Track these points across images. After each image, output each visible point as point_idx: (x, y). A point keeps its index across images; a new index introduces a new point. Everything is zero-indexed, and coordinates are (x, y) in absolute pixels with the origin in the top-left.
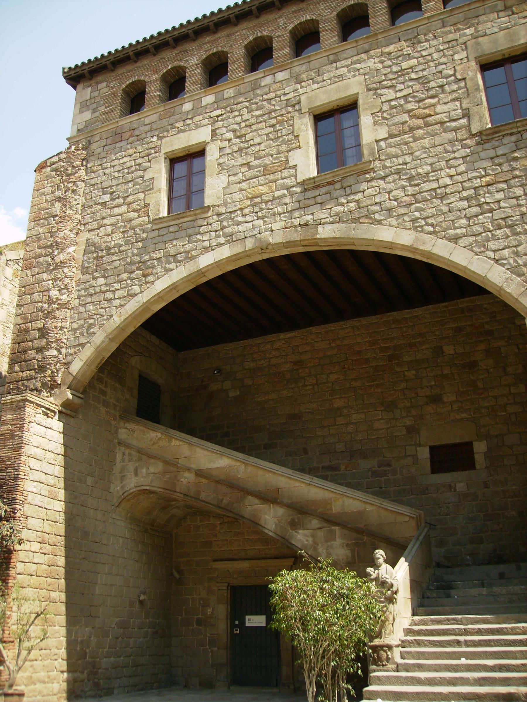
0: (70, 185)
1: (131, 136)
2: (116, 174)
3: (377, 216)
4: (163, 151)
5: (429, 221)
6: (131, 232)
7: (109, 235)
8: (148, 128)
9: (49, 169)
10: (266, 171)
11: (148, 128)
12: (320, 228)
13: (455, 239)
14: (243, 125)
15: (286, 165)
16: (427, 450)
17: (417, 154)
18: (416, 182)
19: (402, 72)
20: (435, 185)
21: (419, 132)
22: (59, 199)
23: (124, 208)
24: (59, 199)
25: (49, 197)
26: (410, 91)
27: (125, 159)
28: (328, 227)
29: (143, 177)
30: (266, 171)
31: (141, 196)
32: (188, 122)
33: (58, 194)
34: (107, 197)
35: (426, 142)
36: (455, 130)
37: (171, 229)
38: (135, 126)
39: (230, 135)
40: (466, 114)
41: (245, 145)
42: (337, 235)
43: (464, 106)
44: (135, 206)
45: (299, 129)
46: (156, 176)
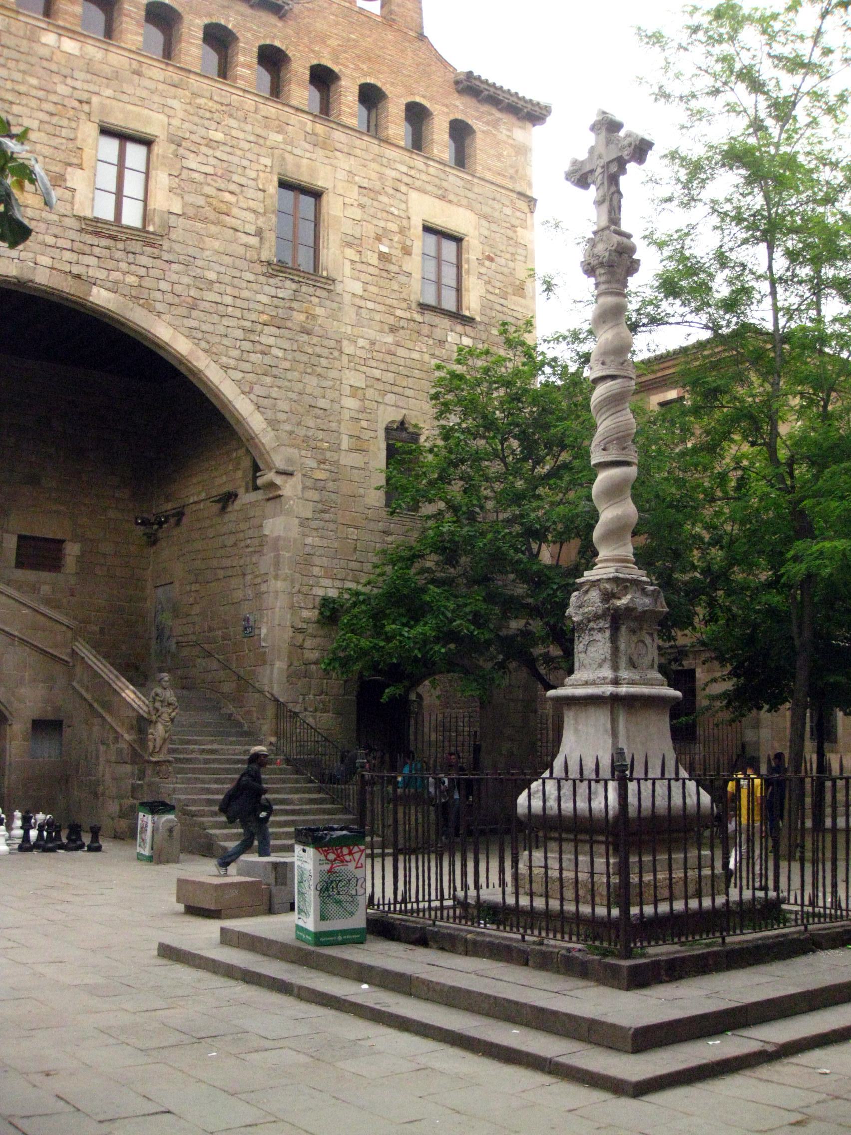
5: (208, 336)
13: (225, 368)
17: (208, 253)
18: (202, 286)
35: (216, 245)
45: (84, 140)
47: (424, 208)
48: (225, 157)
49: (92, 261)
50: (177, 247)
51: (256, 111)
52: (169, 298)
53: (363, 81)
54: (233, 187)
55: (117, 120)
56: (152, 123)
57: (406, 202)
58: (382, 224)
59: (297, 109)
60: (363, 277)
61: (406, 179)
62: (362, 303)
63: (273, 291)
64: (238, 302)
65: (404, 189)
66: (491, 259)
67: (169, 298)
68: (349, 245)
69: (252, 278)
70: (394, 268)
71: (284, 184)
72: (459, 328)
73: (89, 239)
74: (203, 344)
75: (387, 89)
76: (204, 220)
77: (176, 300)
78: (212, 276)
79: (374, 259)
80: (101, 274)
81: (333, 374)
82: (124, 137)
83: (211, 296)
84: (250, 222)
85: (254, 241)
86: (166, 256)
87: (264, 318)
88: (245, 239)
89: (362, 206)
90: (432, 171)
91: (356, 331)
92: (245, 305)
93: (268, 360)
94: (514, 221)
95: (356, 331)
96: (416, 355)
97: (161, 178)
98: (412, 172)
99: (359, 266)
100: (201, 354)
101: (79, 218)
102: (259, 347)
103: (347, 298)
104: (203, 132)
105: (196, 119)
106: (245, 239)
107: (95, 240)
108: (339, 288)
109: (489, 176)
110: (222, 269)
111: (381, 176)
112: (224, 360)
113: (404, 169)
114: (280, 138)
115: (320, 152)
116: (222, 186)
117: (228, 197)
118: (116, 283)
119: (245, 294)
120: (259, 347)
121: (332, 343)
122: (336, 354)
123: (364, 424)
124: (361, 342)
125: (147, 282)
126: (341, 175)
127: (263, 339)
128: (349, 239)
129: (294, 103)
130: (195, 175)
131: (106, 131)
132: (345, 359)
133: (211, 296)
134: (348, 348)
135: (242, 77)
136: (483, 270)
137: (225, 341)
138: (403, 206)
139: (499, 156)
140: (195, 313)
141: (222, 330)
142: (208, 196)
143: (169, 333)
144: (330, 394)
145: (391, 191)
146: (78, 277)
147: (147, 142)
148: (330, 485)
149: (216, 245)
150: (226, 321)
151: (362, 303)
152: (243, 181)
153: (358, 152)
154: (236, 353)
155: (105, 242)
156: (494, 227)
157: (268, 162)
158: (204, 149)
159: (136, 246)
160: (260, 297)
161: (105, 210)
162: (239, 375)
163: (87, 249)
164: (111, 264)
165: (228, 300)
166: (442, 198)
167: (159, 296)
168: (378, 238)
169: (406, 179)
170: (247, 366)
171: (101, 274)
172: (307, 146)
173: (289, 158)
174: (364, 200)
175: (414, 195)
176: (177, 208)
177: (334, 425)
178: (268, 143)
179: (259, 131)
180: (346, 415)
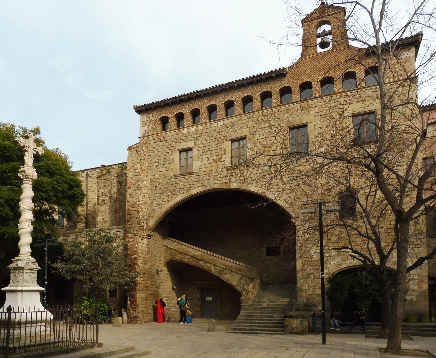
0: (142, 158)
1: (164, 140)
2: (160, 155)
4: (177, 148)
8: (170, 138)
9: (133, 150)
10: (215, 161)
11: (170, 138)
14: (206, 142)
16: (265, 248)
22: (138, 163)
24: (138, 163)
25: (135, 161)
27: (163, 150)
32: (185, 138)
33: (138, 161)
34: (157, 164)
39: (202, 146)
41: (206, 150)
46: (175, 158)
56: (245, 132)
71: (291, 129)
104: (260, 127)
116: (269, 140)
130: (259, 141)
142: (263, 145)
146: (227, 183)
158: (262, 132)
167: (250, 179)
173: (291, 120)
178: (283, 119)
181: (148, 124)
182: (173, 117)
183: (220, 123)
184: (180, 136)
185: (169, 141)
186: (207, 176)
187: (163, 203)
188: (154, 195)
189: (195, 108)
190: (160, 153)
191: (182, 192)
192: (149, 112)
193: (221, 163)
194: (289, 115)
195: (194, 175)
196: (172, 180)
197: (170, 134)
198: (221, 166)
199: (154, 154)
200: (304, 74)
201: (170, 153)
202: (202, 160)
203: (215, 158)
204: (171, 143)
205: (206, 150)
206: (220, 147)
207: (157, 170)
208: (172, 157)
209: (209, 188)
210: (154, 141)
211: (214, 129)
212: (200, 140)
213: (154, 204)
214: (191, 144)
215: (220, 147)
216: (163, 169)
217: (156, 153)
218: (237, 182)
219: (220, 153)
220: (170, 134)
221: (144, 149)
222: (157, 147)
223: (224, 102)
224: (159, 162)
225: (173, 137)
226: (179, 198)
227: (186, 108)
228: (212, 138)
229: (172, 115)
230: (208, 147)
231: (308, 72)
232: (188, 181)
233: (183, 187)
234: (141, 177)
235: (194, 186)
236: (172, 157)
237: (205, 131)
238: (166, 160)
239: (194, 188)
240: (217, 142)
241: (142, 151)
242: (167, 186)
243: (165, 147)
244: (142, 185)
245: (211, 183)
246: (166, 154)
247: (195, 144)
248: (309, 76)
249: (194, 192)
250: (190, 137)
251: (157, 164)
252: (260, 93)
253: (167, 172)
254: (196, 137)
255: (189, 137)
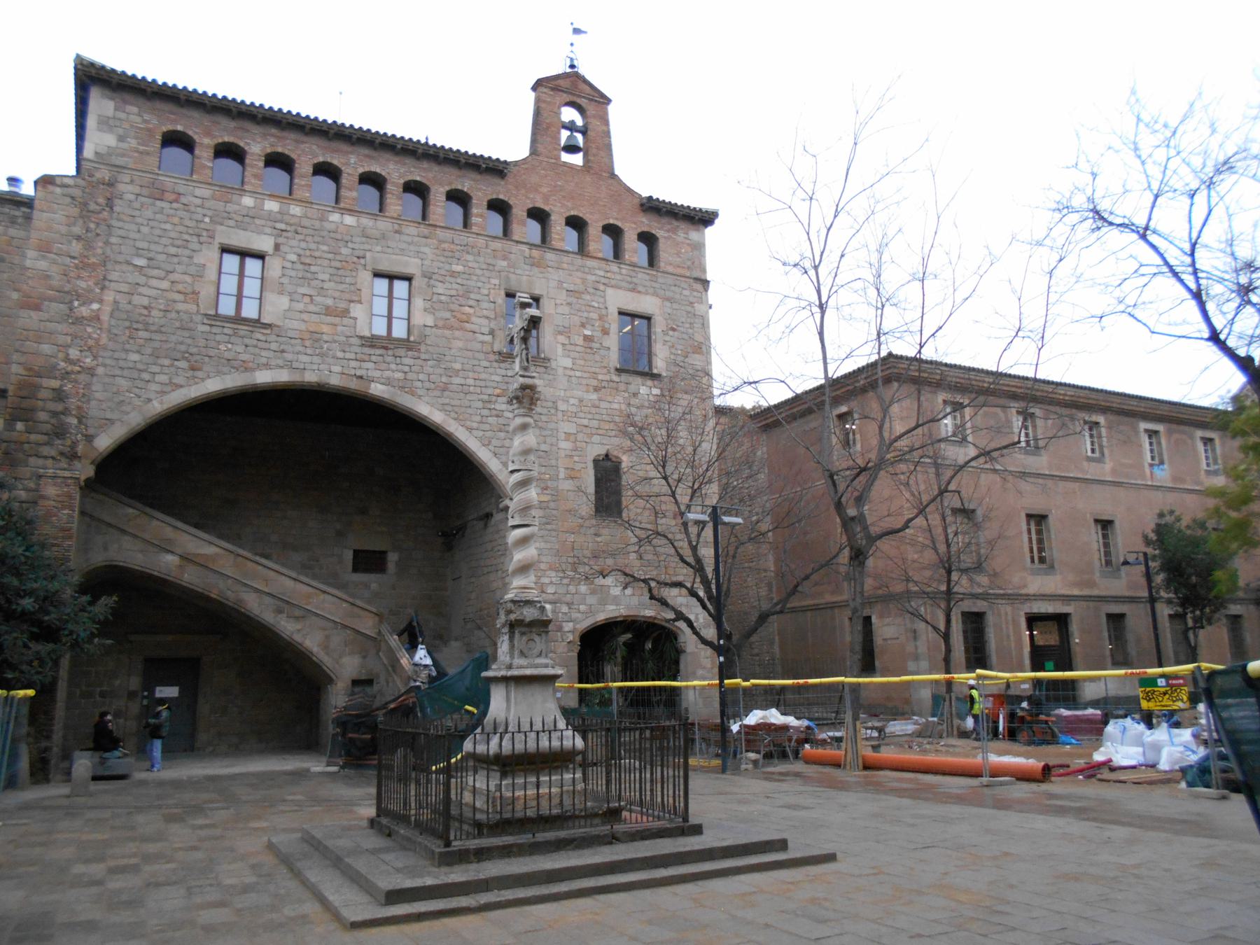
0: (92, 226)
1: (176, 201)
2: (157, 239)
3: (420, 392)
5: (456, 409)
6: (173, 315)
7: (145, 308)
8: (198, 202)
10: (328, 311)
11: (198, 202)
12: (373, 385)
13: (470, 429)
14: (308, 253)
15: (345, 313)
19: (453, 274)
20: (462, 381)
21: (457, 333)
23: (165, 285)
26: (454, 293)
27: (168, 226)
28: (380, 387)
29: (191, 257)
30: (328, 311)
31: (188, 279)
32: (248, 220)
36: (482, 342)
37: (226, 331)
38: (181, 191)
39: (294, 257)
40: (492, 333)
41: (309, 275)
42: (386, 396)
43: (492, 325)
44: (180, 287)
47: (618, 299)
48: (465, 282)
49: (370, 365)
50: (430, 349)
51: (487, 247)
52: (427, 385)
53: (568, 214)
54: (471, 303)
55: (384, 266)
56: (411, 265)
57: (604, 297)
58: (585, 314)
59: (517, 242)
60: (572, 354)
61: (603, 280)
62: (572, 373)
63: (503, 372)
64: (478, 383)
65: (602, 287)
66: (674, 330)
67: (427, 385)
68: (560, 333)
69: (487, 364)
70: (595, 345)
72: (649, 383)
73: (367, 350)
74: (453, 414)
75: (587, 217)
76: (451, 328)
77: (433, 386)
78: (458, 366)
79: (580, 341)
80: (377, 374)
81: (552, 426)
82: (391, 277)
83: (457, 380)
84: (484, 326)
85: (488, 338)
86: (423, 356)
87: (498, 391)
88: (481, 338)
89: (569, 304)
90: (624, 271)
91: (568, 394)
92: (482, 384)
93: (501, 421)
94: (691, 299)
95: (568, 394)
96: (616, 406)
97: (418, 303)
98: (609, 275)
99: (569, 347)
100: (452, 422)
101: (362, 337)
102: (494, 412)
103: (560, 371)
104: (447, 267)
105: (443, 259)
106: (481, 338)
107: (372, 351)
108: (553, 364)
109: (670, 269)
110: (465, 361)
111: (584, 280)
112: (468, 423)
113: (602, 273)
114: (505, 263)
115: (536, 270)
117: (467, 309)
118: (388, 378)
119: (483, 376)
120: (494, 412)
121: (550, 404)
122: (553, 411)
123: (576, 459)
124: (572, 401)
125: (410, 376)
126: (553, 284)
127: (498, 407)
128: (561, 329)
129: (516, 237)
130: (443, 298)
131: (377, 275)
132: (560, 414)
133: (457, 380)
134: (562, 406)
135: (476, 224)
136: (667, 338)
137: (469, 411)
138: (602, 300)
139: (678, 254)
140: (446, 393)
141: (467, 403)
143: (428, 410)
144: (548, 440)
145: (592, 291)
146: (361, 377)
147: (409, 279)
148: (552, 505)
149: (460, 344)
150: (468, 397)
151: (572, 373)
152: (478, 297)
153: (565, 266)
154: (478, 418)
155: (379, 352)
156: (675, 306)
157: (497, 282)
158: (448, 278)
159: (401, 352)
160: (494, 377)
161: (380, 329)
162: (481, 433)
163: (366, 358)
164: (384, 366)
165: (471, 382)
166: (633, 290)
167: (419, 384)
168: (583, 325)
169: (603, 280)
170: (487, 427)
171: (377, 374)
172: (526, 267)
173: (512, 277)
174: (570, 300)
175: (610, 291)
176: (430, 322)
177: (553, 462)
179: (490, 261)
180: (562, 454)
181: (121, 131)
182: (208, 146)
183: (349, 220)
184: (228, 209)
185: (193, 209)
186: (308, 343)
187: (154, 387)
188: (123, 356)
189: (280, 150)
190: (157, 232)
191: (225, 369)
192: (127, 97)
193: (346, 321)
194: (509, 266)
195: (268, 331)
196: (191, 325)
197: (198, 192)
198: (348, 331)
199: (134, 227)
200: (536, 190)
201: (195, 246)
202: (296, 297)
203: (330, 302)
204: (199, 217)
205: (309, 275)
206: (348, 280)
207: (142, 280)
208: (199, 259)
209: (311, 377)
210: (137, 190)
211: (332, 227)
212: (294, 243)
213: (122, 382)
214: (264, 243)
215: (348, 280)
216: (165, 285)
217: (145, 230)
218: (388, 382)
219: (347, 296)
220: (198, 192)
221: (101, 200)
222: (149, 213)
223: (361, 170)
224: (150, 259)
225: (207, 204)
226: (213, 385)
227: (254, 140)
228: (325, 248)
229: (207, 141)
230: (313, 269)
231: (545, 190)
232: (247, 341)
233: (227, 355)
234: (83, 284)
235: (264, 360)
236: (199, 259)
237: (306, 222)
238: (176, 260)
239: (267, 366)
240: (338, 264)
241: (92, 206)
242: (173, 338)
243: (176, 220)
244: (84, 311)
245: (315, 367)
246: (179, 243)
247: (277, 247)
248: (546, 198)
249: (264, 378)
250: (263, 222)
251: (141, 262)
252: (448, 188)
253: (180, 297)
254: (283, 229)
255: (257, 222)
